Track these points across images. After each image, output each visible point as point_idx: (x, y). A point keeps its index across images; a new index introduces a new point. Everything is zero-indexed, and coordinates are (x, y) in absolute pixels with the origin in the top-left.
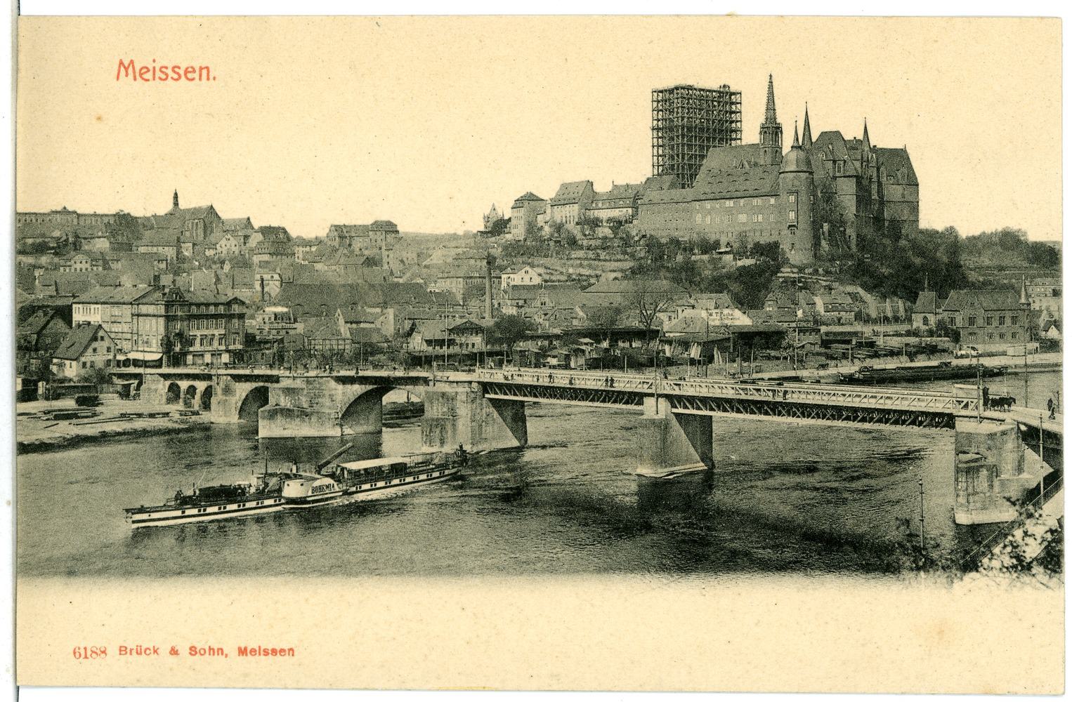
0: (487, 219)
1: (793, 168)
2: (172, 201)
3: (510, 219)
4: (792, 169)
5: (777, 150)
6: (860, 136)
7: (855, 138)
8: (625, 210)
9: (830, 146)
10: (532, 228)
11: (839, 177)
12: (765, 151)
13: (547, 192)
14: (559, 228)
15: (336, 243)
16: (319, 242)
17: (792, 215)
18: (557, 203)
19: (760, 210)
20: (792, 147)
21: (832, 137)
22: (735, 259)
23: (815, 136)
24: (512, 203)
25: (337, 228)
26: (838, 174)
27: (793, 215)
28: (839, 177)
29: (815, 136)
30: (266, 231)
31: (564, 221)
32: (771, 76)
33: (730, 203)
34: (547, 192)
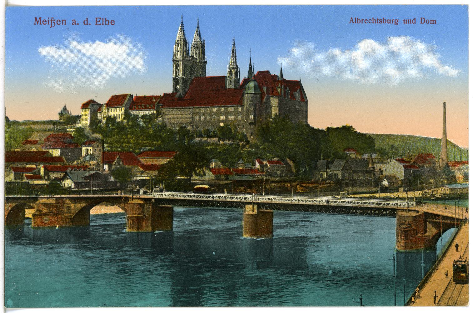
0: (61, 114)
3: (81, 115)
4: (252, 92)
5: (237, 81)
6: (278, 74)
7: (274, 74)
10: (94, 122)
12: (231, 81)
13: (103, 100)
14: (111, 120)
17: (252, 117)
19: (231, 114)
21: (264, 74)
22: (219, 141)
23: (256, 73)
24: (81, 105)
27: (252, 117)
31: (115, 115)
32: (234, 39)
34: (103, 100)
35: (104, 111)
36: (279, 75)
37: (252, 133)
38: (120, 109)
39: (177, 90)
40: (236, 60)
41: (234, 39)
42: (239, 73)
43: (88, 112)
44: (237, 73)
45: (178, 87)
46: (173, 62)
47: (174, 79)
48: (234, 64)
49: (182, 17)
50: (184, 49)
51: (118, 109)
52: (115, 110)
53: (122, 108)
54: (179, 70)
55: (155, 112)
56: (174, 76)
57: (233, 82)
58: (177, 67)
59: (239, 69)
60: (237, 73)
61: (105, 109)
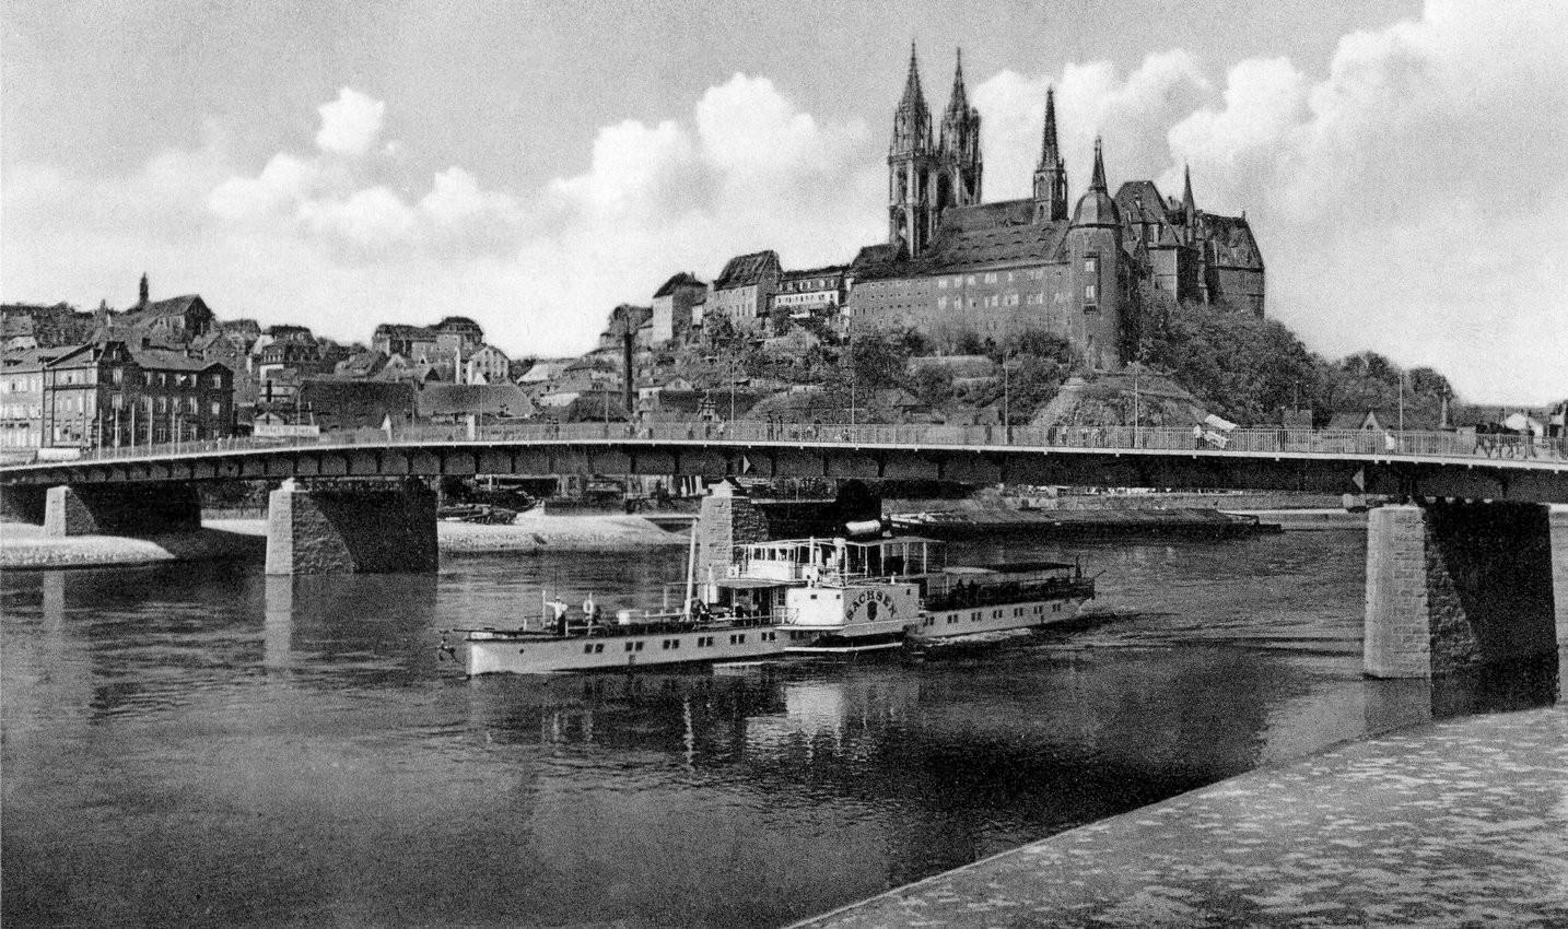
1: (1094, 220)
2: (137, 291)
7: (1170, 198)
8: (827, 294)
9: (1138, 203)
11: (1155, 248)
15: (386, 348)
16: (360, 349)
17: (1091, 292)
18: (726, 281)
20: (1091, 189)
23: (1112, 191)
25: (387, 330)
26: (1150, 244)
28: (1155, 248)
29: (1112, 191)
30: (276, 331)
32: (1050, 93)
33: (991, 279)
34: (709, 272)
35: (709, 300)
36: (1179, 196)
37: (1090, 337)
39: (900, 238)
41: (1050, 93)
42: (1066, 185)
43: (668, 302)
44: (1060, 181)
45: (903, 232)
47: (893, 210)
55: (836, 294)
56: (893, 203)
58: (903, 176)
59: (1064, 175)
60: (1059, 188)
61: (713, 301)
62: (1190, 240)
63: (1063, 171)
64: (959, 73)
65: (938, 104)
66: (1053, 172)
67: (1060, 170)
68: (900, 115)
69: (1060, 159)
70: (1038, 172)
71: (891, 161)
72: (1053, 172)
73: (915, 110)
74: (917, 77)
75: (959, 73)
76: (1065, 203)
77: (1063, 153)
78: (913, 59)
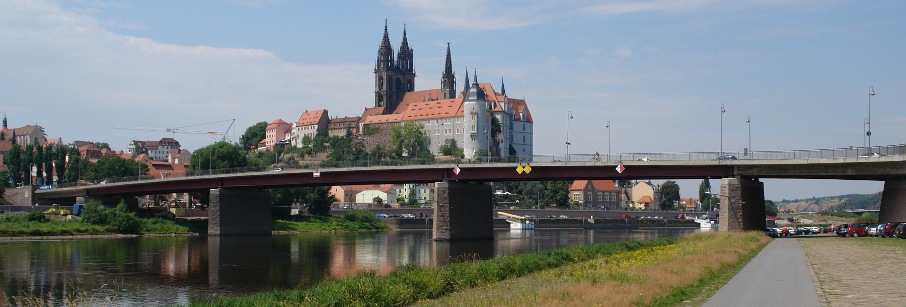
32: (449, 44)
37: (474, 148)
38: (313, 126)
40: (451, 68)
41: (449, 44)
45: (382, 103)
46: (375, 74)
48: (449, 73)
49: (386, 21)
50: (388, 58)
51: (310, 127)
52: (306, 129)
53: (315, 126)
54: (382, 83)
57: (448, 96)
58: (381, 79)
62: (506, 109)
63: (454, 78)
64: (405, 34)
65: (396, 47)
66: (449, 78)
67: (453, 76)
68: (380, 53)
69: (453, 71)
70: (443, 78)
71: (376, 72)
72: (449, 78)
73: (386, 48)
74: (388, 35)
75: (405, 34)
76: (455, 91)
77: (454, 69)
78: (386, 27)
